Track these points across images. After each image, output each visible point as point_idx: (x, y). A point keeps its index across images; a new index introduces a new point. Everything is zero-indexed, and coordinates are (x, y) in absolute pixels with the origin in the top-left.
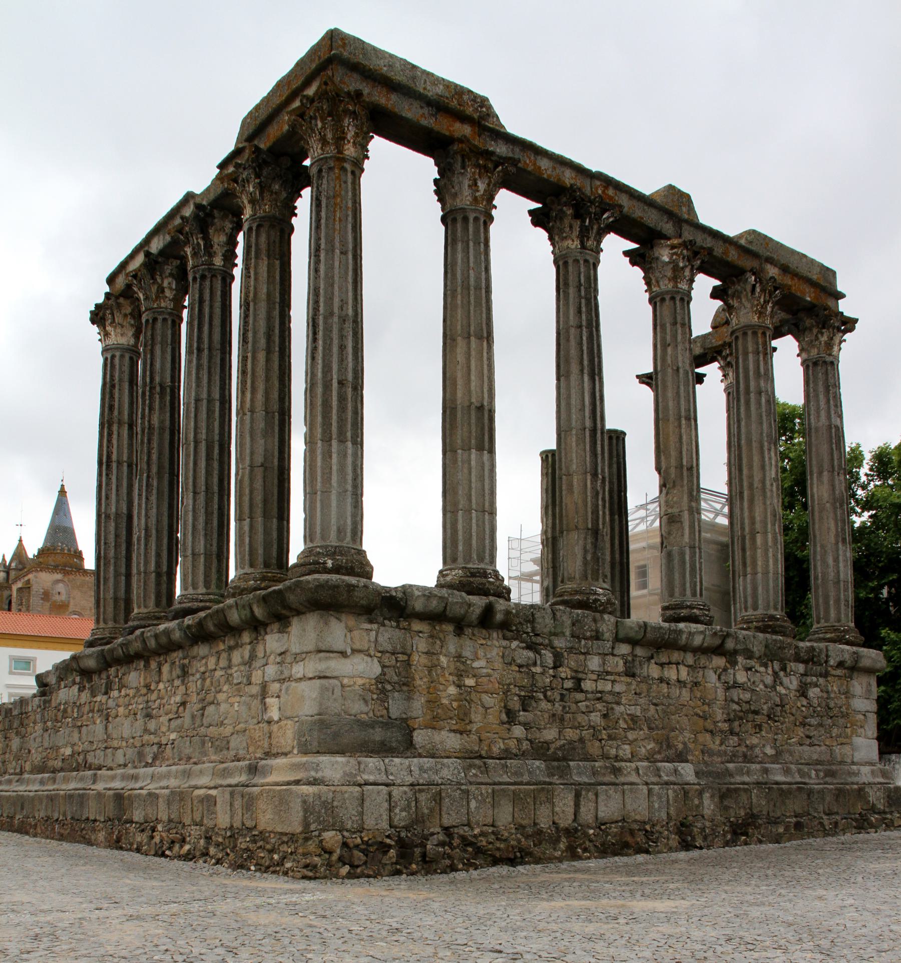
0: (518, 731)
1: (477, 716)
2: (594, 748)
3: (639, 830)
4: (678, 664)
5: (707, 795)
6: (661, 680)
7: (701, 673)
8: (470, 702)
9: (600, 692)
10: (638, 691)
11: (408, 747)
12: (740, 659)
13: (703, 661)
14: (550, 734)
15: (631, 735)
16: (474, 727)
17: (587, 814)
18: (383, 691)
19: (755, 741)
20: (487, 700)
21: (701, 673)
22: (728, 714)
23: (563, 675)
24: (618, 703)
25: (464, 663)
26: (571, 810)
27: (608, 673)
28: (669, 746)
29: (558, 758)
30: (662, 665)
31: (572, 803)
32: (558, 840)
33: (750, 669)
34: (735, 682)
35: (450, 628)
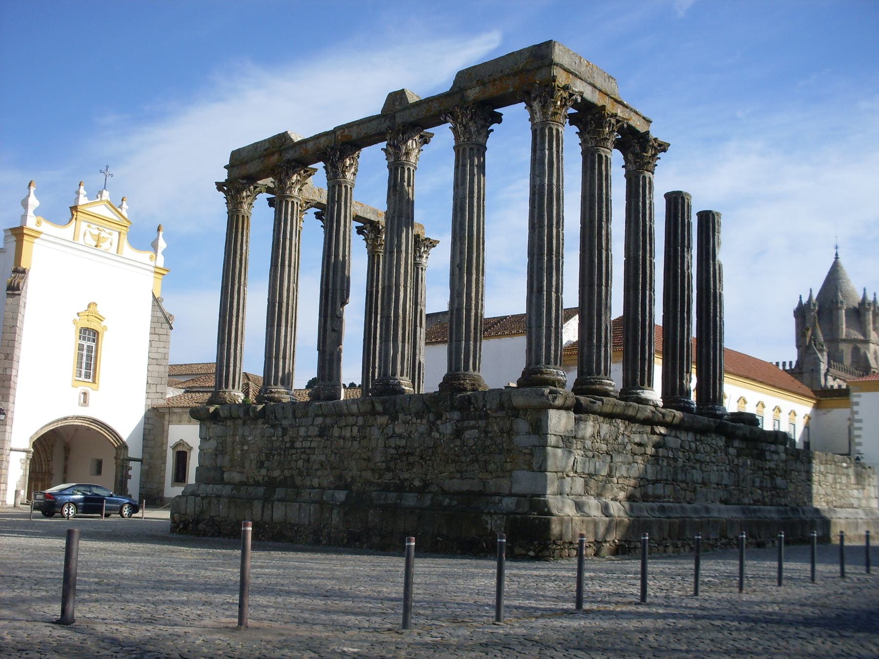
0: (264, 472)
1: (247, 465)
2: (298, 481)
5: (335, 511)
6: (340, 437)
12: (401, 416)
14: (276, 473)
15: (319, 473)
16: (245, 470)
18: (216, 455)
19: (406, 475)
22: (386, 457)
24: (314, 454)
26: (259, 513)
27: (309, 436)
30: (341, 428)
35: (240, 422)
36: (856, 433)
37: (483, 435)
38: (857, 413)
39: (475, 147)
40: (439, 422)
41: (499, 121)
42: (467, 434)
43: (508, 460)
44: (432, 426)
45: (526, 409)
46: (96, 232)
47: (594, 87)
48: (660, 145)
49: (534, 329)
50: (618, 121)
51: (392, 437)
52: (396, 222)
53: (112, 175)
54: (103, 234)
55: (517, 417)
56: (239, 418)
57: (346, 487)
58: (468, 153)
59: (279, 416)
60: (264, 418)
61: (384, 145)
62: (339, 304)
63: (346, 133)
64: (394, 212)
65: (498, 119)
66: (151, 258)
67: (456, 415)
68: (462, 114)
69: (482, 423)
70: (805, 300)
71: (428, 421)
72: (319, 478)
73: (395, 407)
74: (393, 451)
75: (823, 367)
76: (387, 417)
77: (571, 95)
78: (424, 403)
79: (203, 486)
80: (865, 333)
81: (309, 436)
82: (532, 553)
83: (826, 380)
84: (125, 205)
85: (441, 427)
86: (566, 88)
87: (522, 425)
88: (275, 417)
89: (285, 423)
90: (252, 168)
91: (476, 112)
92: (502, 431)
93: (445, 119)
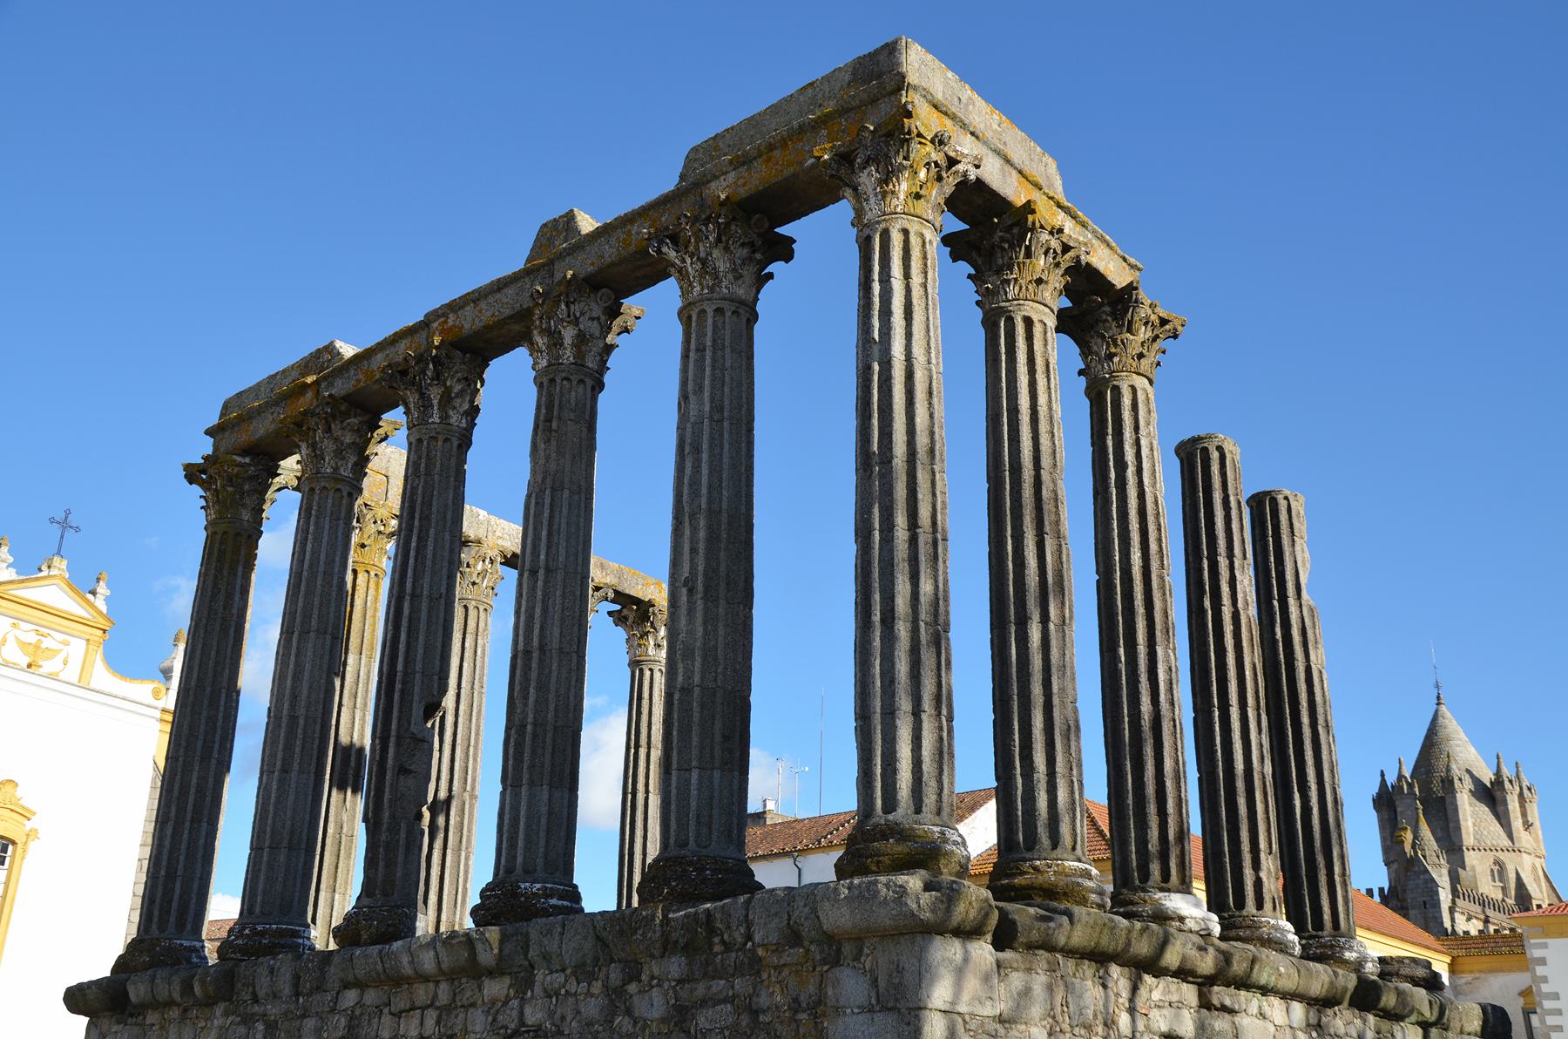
4: (423, 1009)
7: (462, 1016)
12: (539, 977)
30: (397, 1015)
36: (1551, 1020)
37: (745, 1020)
38: (1545, 979)
39: (725, 305)
40: (632, 988)
41: (788, 256)
42: (703, 1020)
44: (617, 999)
45: (859, 939)
46: (33, 638)
47: (1007, 161)
48: (1164, 322)
50: (1066, 248)
52: (547, 501)
53: (77, 529)
54: (46, 643)
55: (836, 961)
58: (710, 321)
59: (261, 994)
60: (230, 1000)
62: (417, 710)
63: (450, 323)
64: (544, 479)
65: (784, 249)
66: (156, 694)
67: (675, 966)
69: (740, 984)
70: (1391, 779)
71: (606, 987)
75: (1445, 897)
76: (507, 980)
77: (952, 162)
80: (1510, 836)
83: (1453, 920)
84: (102, 589)
85: (636, 999)
86: (939, 141)
87: (850, 986)
88: (254, 994)
89: (273, 1010)
90: (262, 428)
91: (727, 225)
93: (659, 251)
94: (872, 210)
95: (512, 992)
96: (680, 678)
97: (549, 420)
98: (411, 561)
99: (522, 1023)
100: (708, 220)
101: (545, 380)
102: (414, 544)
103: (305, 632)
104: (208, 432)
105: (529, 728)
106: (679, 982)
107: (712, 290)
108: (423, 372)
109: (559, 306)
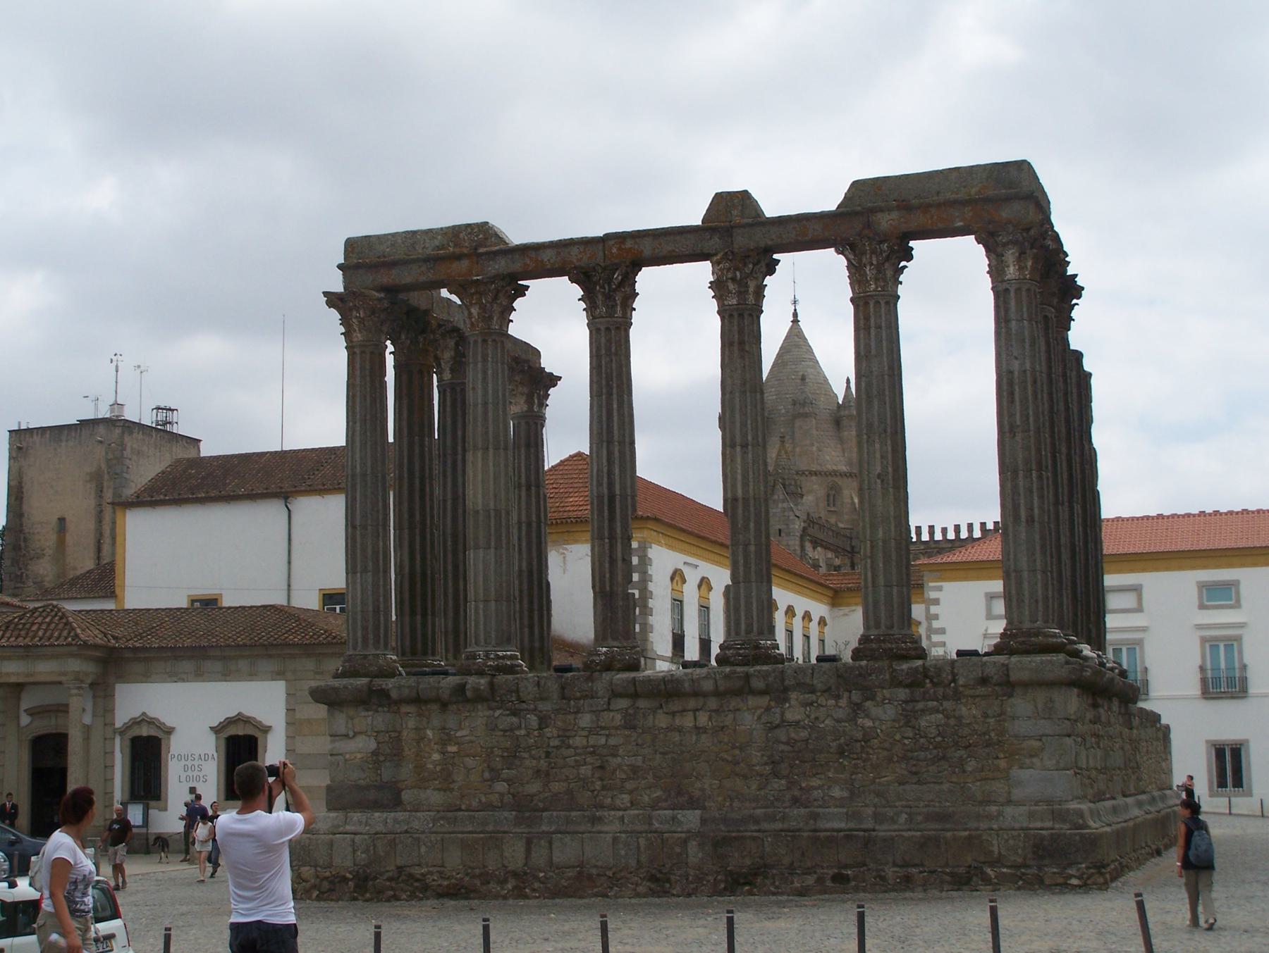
0: (501, 787)
1: (459, 778)
3: (598, 875)
4: (696, 710)
6: (670, 729)
8: (453, 764)
9: (593, 746)
10: (640, 741)
11: (396, 803)
12: (793, 695)
13: (734, 702)
14: (533, 788)
15: (629, 785)
17: (539, 856)
20: (469, 761)
21: (731, 716)
23: (549, 735)
24: (615, 756)
25: (448, 734)
27: (603, 728)
28: (679, 793)
29: (524, 807)
31: (523, 849)
32: (505, 881)
33: (811, 704)
34: (783, 721)
37: (952, 722)
38: (936, 617)
40: (868, 704)
43: (1001, 755)
44: (857, 708)
45: (1026, 685)
49: (1025, 575)
51: (777, 726)
55: (1011, 696)
56: (437, 700)
57: (693, 804)
61: (702, 272)
64: (744, 384)
67: (902, 693)
68: (873, 252)
69: (948, 705)
72: (630, 792)
73: (783, 680)
74: (782, 747)
78: (839, 676)
79: (356, 816)
81: (603, 728)
82: (1074, 882)
89: (545, 707)
92: (986, 715)
94: (1011, 272)
95: (773, 704)
96: (880, 534)
97: (742, 343)
98: (615, 419)
99: (783, 721)
100: (881, 242)
101: (735, 314)
102: (615, 406)
103: (496, 448)
104: (340, 267)
105: (752, 548)
106: (906, 702)
107: (883, 287)
108: (609, 280)
109: (745, 265)
